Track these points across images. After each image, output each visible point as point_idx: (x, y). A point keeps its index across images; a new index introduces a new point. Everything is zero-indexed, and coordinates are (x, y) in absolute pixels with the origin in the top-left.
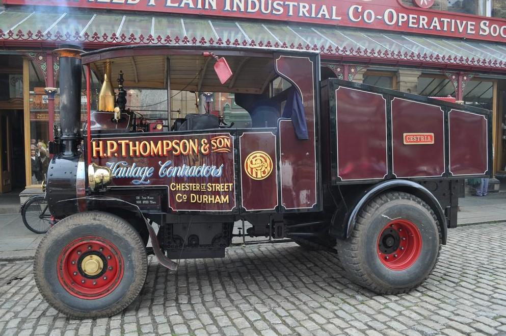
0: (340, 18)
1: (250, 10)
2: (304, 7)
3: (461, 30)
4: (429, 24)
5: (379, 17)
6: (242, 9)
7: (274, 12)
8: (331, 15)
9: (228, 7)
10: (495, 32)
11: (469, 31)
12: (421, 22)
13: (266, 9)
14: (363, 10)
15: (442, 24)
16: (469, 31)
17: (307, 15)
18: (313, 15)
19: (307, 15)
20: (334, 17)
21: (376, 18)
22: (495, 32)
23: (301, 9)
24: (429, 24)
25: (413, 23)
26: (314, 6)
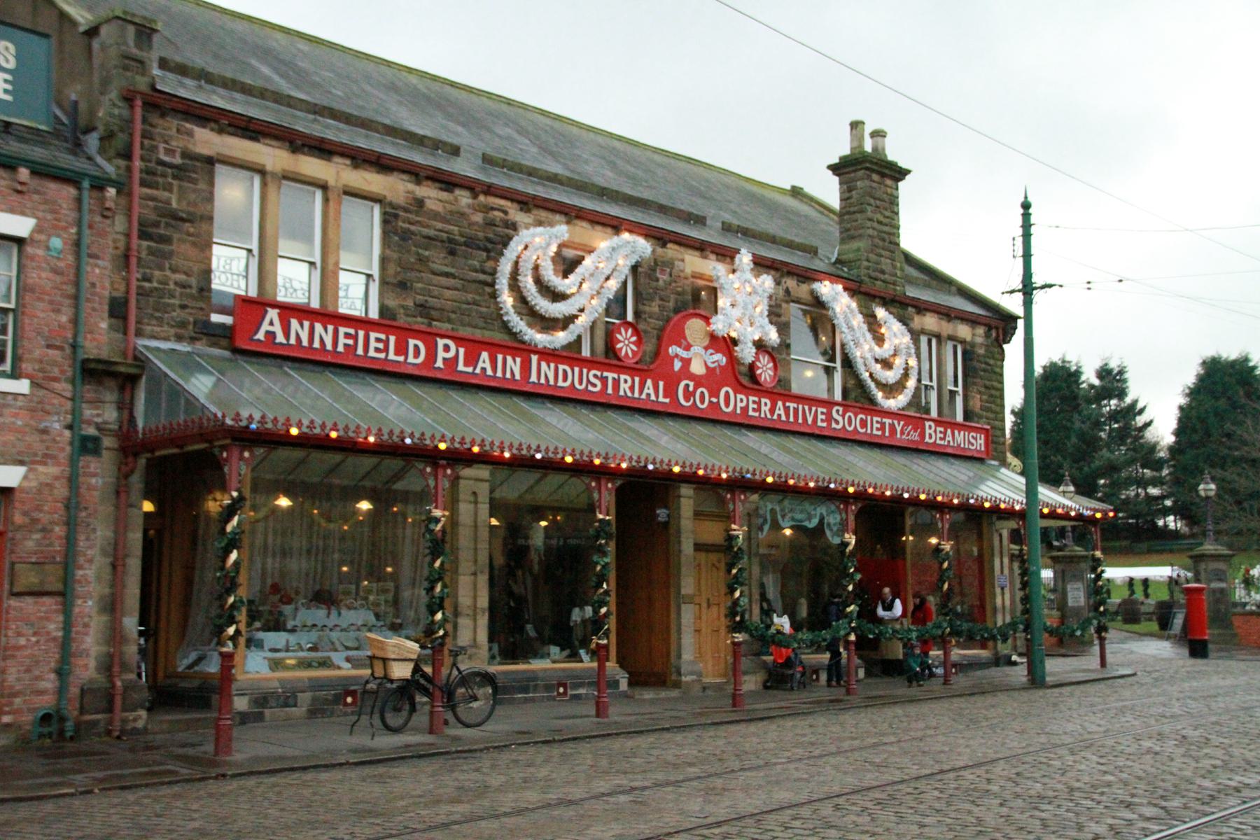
0: (667, 400)
1: (560, 383)
2: (626, 381)
3: (810, 420)
4: (772, 411)
5: (714, 400)
6: (552, 382)
7: (590, 388)
8: (657, 396)
9: (534, 378)
10: (850, 424)
11: (820, 424)
12: (763, 408)
13: (581, 383)
14: (696, 389)
15: (787, 409)
16: (820, 424)
17: (629, 394)
18: (636, 395)
19: (629, 394)
20: (661, 399)
21: (710, 402)
22: (850, 424)
23: (622, 385)
24: (772, 411)
25: (754, 410)
26: (637, 379)
